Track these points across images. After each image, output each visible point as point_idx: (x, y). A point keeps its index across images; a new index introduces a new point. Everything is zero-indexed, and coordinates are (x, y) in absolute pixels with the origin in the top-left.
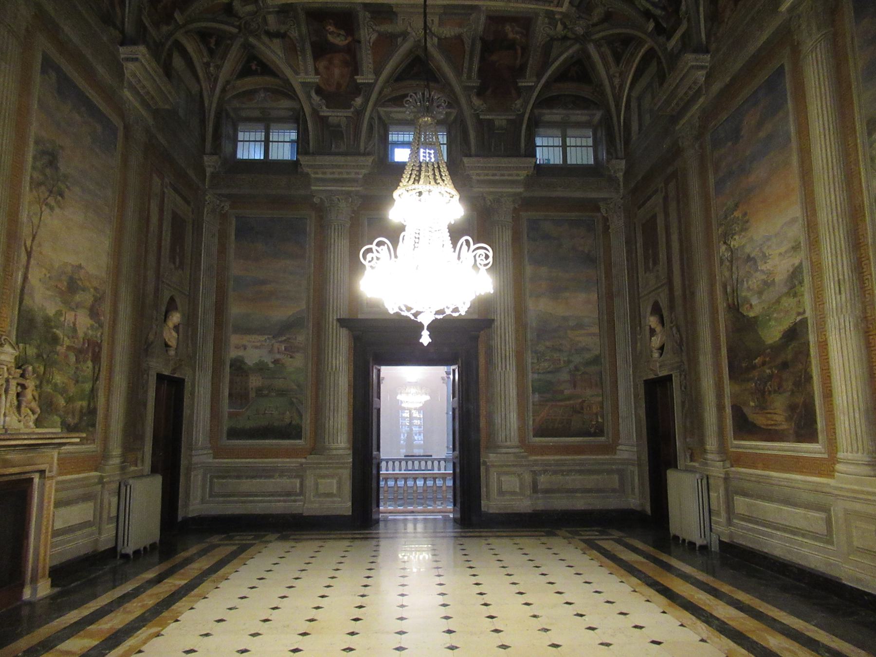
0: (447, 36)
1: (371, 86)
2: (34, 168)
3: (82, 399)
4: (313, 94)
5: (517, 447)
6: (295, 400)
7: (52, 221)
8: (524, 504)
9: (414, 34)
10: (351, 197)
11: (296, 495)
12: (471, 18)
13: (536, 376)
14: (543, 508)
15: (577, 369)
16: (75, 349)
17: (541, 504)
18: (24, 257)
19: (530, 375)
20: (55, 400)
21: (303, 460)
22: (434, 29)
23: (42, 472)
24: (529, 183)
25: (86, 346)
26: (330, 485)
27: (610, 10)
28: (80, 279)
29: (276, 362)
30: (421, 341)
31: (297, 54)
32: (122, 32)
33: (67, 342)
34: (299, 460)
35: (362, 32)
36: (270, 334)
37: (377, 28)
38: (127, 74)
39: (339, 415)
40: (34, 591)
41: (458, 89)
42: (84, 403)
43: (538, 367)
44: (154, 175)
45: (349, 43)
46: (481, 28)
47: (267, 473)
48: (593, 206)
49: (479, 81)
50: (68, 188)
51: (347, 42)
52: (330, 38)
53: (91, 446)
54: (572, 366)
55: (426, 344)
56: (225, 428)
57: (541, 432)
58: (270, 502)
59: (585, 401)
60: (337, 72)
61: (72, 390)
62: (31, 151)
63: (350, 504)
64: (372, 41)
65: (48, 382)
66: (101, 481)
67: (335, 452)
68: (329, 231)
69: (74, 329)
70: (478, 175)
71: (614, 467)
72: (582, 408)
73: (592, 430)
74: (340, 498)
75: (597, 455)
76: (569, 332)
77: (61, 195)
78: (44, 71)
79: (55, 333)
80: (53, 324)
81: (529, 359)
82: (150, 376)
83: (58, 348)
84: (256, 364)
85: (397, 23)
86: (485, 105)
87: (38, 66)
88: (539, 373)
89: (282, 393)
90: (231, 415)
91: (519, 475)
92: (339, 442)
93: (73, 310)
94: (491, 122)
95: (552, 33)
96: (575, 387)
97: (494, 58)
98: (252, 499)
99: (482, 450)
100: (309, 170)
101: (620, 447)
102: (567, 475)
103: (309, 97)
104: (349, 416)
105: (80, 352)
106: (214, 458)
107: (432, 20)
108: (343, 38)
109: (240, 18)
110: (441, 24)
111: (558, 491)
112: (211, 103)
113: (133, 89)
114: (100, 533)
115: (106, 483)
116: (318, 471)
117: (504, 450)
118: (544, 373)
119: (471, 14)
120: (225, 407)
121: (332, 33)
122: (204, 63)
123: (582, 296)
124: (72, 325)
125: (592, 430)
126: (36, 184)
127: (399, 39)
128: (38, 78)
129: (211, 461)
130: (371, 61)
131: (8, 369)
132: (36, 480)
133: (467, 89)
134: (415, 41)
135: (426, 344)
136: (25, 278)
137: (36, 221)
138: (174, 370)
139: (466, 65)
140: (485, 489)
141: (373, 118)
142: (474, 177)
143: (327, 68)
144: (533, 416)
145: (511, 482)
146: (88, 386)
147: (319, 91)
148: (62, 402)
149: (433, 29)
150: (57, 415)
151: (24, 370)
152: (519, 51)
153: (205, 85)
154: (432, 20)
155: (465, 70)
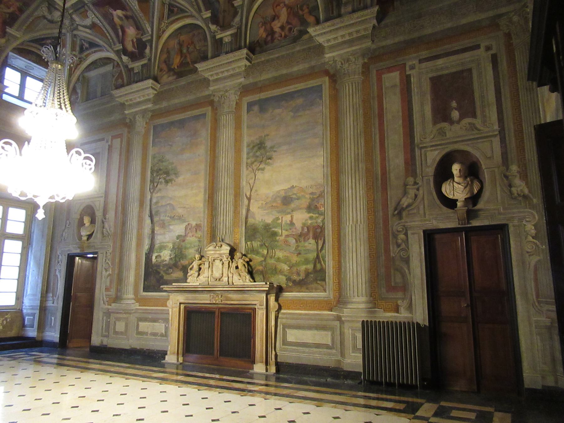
16: (293, 235)
18: (246, 202)
25: (306, 230)
33: (285, 233)
42: (310, 267)
61: (295, 259)
65: (271, 258)
69: (292, 224)
77: (270, 159)
82: (409, 235)
83: (278, 238)
93: (289, 213)
105: (301, 236)
124: (289, 222)
136: (248, 210)
146: (312, 256)
148: (286, 267)
150: (281, 275)
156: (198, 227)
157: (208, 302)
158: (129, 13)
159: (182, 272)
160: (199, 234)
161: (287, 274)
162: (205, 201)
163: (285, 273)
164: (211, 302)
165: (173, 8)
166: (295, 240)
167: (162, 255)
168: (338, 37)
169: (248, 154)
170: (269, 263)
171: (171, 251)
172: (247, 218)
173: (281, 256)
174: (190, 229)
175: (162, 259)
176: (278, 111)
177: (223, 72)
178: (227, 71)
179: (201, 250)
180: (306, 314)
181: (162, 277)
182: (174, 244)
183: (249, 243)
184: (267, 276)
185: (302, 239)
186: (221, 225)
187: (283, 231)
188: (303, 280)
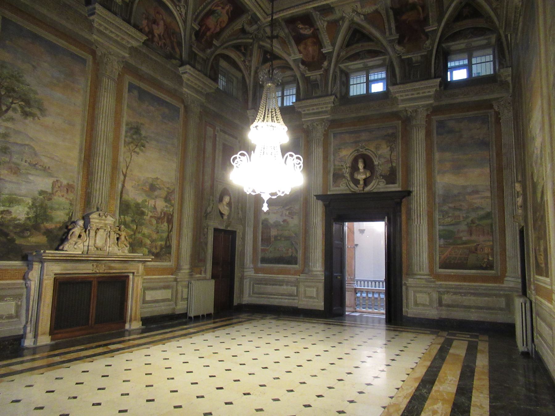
1: (331, 53)
2: (126, 137)
3: (161, 241)
4: (300, 65)
5: (429, 275)
6: (294, 243)
7: (139, 159)
8: (433, 313)
9: (348, 17)
10: (324, 122)
11: (295, 296)
13: (441, 228)
14: (446, 317)
15: (473, 222)
16: (155, 217)
17: (444, 314)
18: (122, 177)
19: (438, 227)
20: (143, 241)
21: (298, 277)
22: (359, 10)
23: (133, 273)
24: (437, 96)
25: (163, 215)
26: (312, 292)
28: (158, 184)
29: (284, 221)
30: (263, 209)
32: (181, 59)
33: (150, 214)
34: (296, 276)
35: (318, 24)
36: (281, 206)
37: (325, 19)
38: (185, 80)
39: (318, 251)
40: (130, 325)
41: (385, 43)
42: (163, 243)
43: (443, 221)
44: (208, 127)
45: (313, 32)
47: (280, 283)
48: (488, 104)
49: (398, 34)
50: (147, 142)
51: (312, 31)
52: (302, 31)
53: (168, 263)
54: (469, 220)
55: (265, 211)
56: (260, 257)
57: (445, 265)
58: (281, 299)
59: (479, 245)
61: (155, 236)
62: (124, 128)
63: (323, 304)
64: (325, 27)
65: (139, 233)
66: (176, 280)
67: (315, 273)
68: (312, 144)
69: (155, 208)
70: (401, 96)
71: (501, 292)
72: (476, 250)
73: (484, 265)
74: (318, 299)
75: (489, 283)
76: (467, 197)
77: (144, 146)
78: (129, 91)
79: (142, 210)
80: (140, 206)
81: (437, 216)
82: (209, 229)
83: (145, 217)
84: (274, 223)
85: (336, 13)
86: (405, 49)
87: (126, 90)
88: (443, 225)
89: (288, 238)
90: (263, 250)
91: (429, 294)
92: (317, 267)
93: (153, 199)
94: (410, 59)
96: (471, 234)
97: (404, 17)
98: (272, 296)
99: (403, 276)
100: (300, 110)
101: (506, 279)
102: (465, 296)
103: (299, 67)
104: (322, 252)
105: (159, 219)
106: (254, 273)
107: (357, 6)
109: (251, 34)
110: (362, 7)
111: (457, 306)
112: (250, 81)
113: (189, 87)
114: (176, 305)
115: (179, 281)
116: (306, 284)
117: (419, 277)
118: (447, 225)
120: (260, 247)
121: (302, 28)
122: (242, 61)
123: (477, 171)
124: (153, 206)
125: (484, 265)
126: (127, 144)
127: (340, 22)
128: (126, 95)
129: (253, 274)
130: (327, 39)
131: (110, 227)
132: (131, 276)
133: (391, 42)
134: (349, 21)
135: (265, 211)
136: (123, 186)
137: (128, 160)
138: (227, 226)
139: (386, 27)
140: (405, 301)
141: (336, 72)
142: (399, 98)
143: (305, 48)
144: (440, 254)
145: (423, 298)
146: (165, 235)
147: (303, 63)
148: (148, 242)
149: (358, 10)
150: (145, 248)
151: (120, 228)
152: (420, 9)
153: (246, 73)
155: (387, 30)
156: (69, 188)
157: (91, 272)
159: (45, 236)
160: (71, 196)
161: (149, 247)
162: (80, 160)
163: (148, 247)
164: (93, 272)
166: (156, 221)
167: (13, 212)
168: (120, 37)
169: (126, 132)
170: (137, 237)
171: (29, 208)
172: (122, 193)
173: (146, 233)
174: (59, 187)
175: (13, 216)
176: (151, 108)
177: (111, 32)
178: (117, 36)
179: (72, 215)
180: (158, 279)
181: (13, 240)
182: (34, 199)
183: (122, 217)
184: (135, 248)
185: (160, 221)
186: (98, 193)
187: (149, 212)
188: (158, 252)
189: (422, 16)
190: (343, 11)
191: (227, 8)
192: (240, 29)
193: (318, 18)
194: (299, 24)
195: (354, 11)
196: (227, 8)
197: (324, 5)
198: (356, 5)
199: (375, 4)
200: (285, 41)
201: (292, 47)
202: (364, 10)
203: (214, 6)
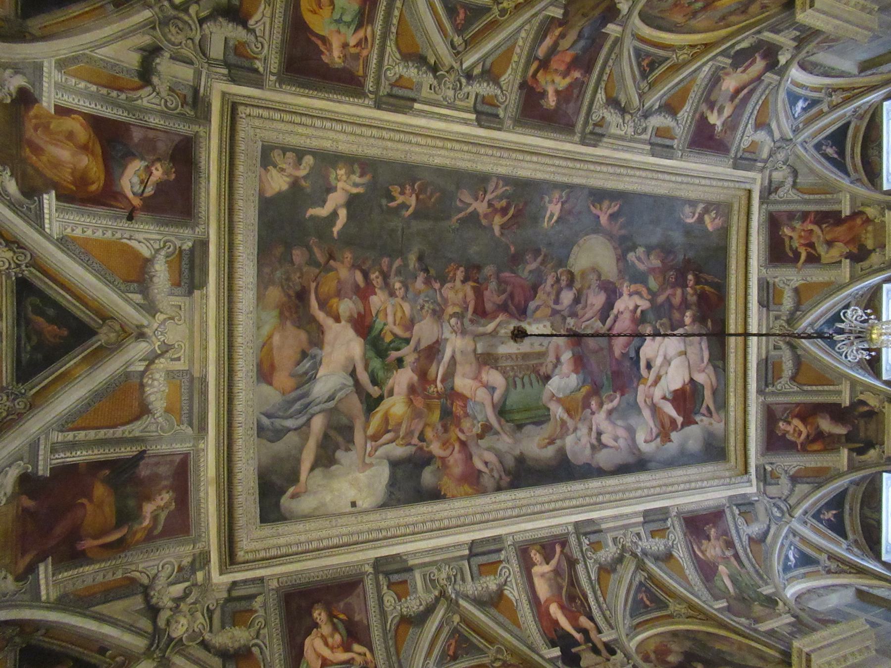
0: (147, 389)
12: (183, 427)
22: (162, 364)
27: (255, 650)
31: (105, 86)
41: (34, 425)
45: (127, 198)
46: (164, 448)
51: (130, 195)
52: (136, 166)
60: (65, 154)
64: (133, 243)
85: (172, 294)
95: (161, 581)
97: (100, 491)
107: (179, 359)
108: (138, 188)
109: (202, 21)
110: (171, 375)
119: (191, 424)
121: (148, 170)
130: (89, 232)
149: (162, 360)
154: (179, 359)
155: (70, 436)
158: (704, 107)
165: (646, 68)
189: (88, 544)
190: (172, 318)
191: (336, 53)
192: (250, 16)
193: (173, 239)
194: (166, 173)
195: (166, 348)
196: (336, 53)
197: (205, 272)
198: (182, 361)
199: (168, 411)
200: (121, 90)
201: (91, 96)
202: (160, 376)
203: (369, 39)
